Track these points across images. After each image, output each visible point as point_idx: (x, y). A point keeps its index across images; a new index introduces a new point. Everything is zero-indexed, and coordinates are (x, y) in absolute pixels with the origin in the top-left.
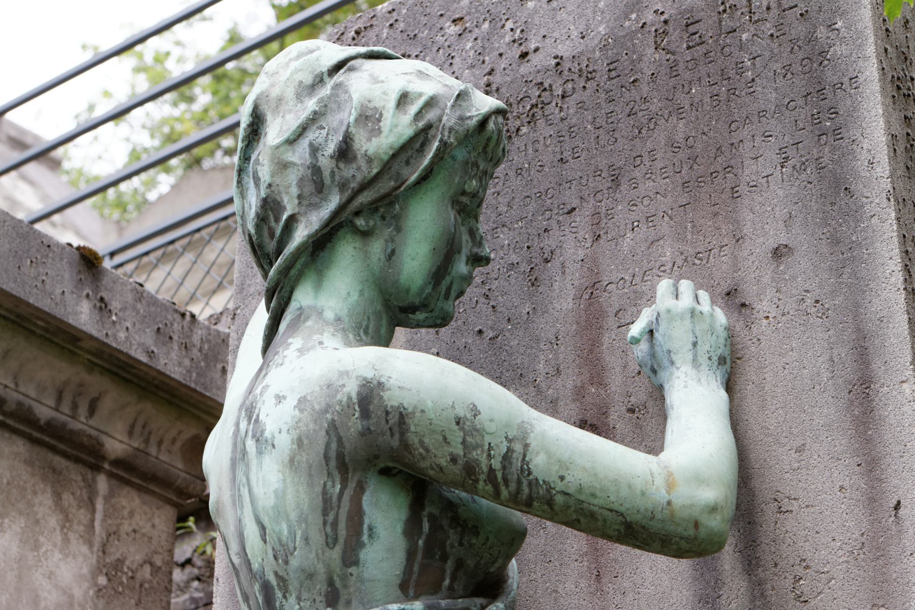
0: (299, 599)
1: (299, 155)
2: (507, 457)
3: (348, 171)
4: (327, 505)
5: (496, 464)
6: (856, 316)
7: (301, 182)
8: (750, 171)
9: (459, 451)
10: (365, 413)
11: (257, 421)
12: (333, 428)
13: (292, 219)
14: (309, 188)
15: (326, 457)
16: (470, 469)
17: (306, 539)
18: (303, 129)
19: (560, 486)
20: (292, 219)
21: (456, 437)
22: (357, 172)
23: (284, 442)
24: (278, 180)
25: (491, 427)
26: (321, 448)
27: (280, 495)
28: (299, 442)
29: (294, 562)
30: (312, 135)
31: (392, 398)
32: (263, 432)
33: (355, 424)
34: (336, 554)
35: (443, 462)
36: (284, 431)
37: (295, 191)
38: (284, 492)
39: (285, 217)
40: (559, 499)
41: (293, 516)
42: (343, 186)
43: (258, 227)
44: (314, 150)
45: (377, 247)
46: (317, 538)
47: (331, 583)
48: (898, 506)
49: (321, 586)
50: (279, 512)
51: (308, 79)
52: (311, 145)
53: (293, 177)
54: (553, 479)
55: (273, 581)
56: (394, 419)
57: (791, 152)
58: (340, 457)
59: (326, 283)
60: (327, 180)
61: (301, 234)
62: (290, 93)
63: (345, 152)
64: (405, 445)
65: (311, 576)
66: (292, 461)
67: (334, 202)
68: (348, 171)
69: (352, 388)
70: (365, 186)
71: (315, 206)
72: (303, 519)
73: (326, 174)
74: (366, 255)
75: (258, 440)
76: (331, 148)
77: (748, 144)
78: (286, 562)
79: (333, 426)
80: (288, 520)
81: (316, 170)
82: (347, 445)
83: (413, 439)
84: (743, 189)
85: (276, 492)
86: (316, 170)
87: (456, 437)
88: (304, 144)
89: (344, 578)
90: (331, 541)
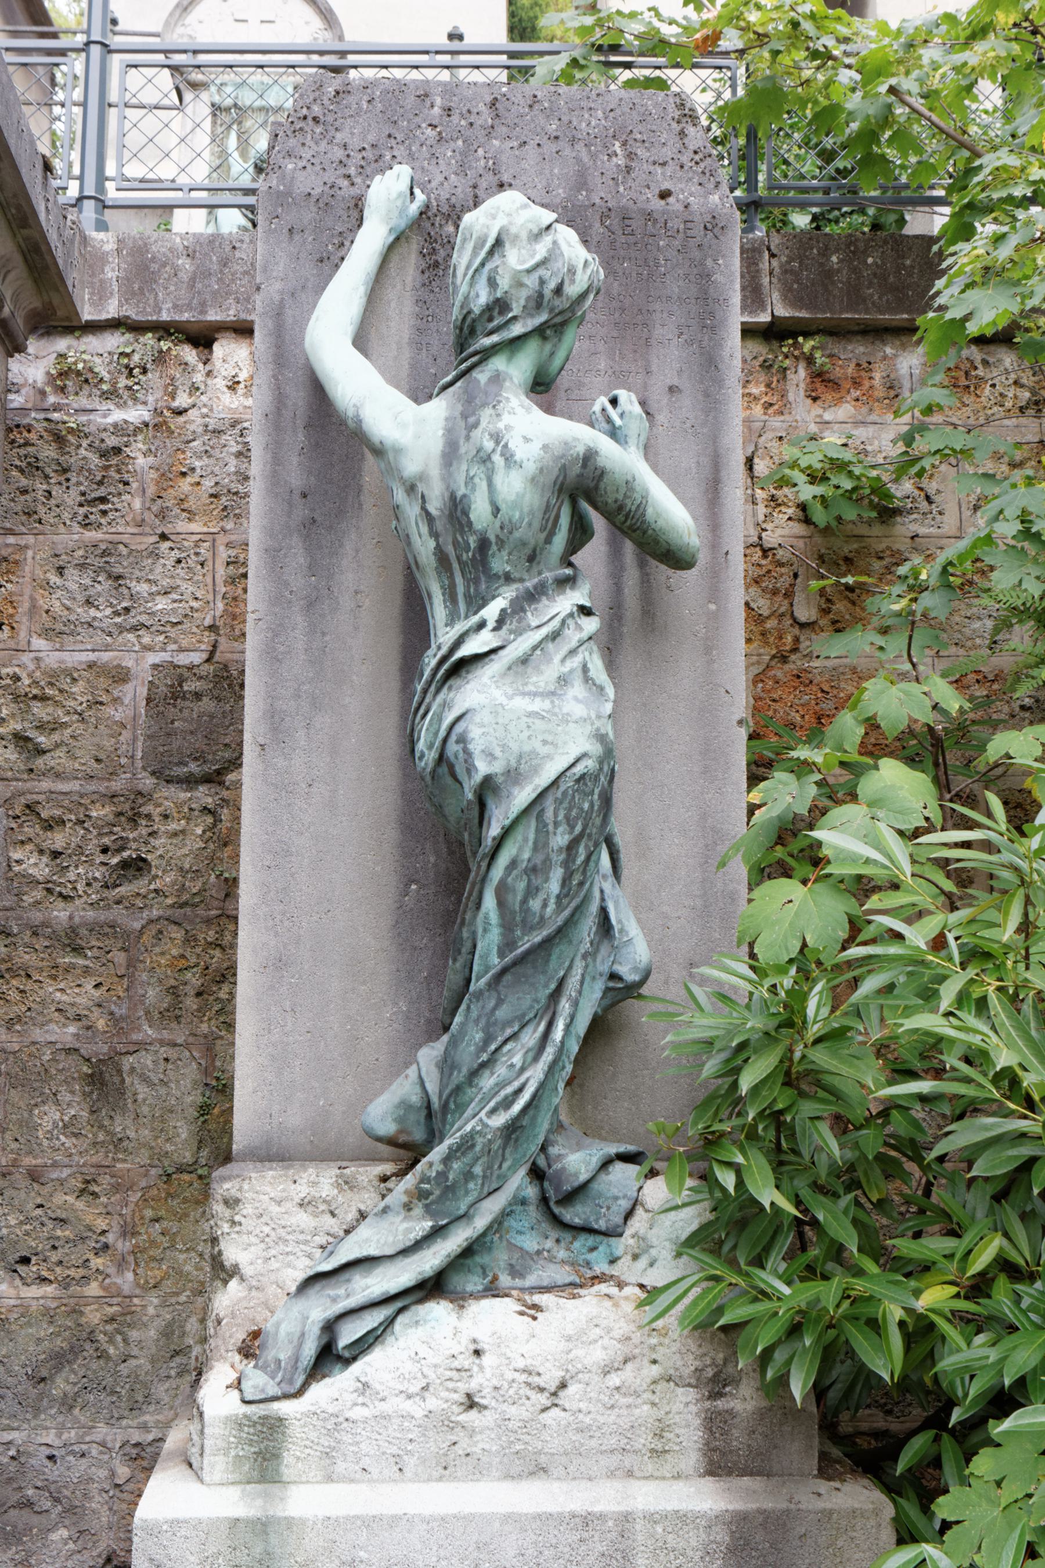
0: (510, 554)
1: (532, 281)
2: (639, 506)
3: (557, 302)
4: (547, 509)
5: (633, 508)
6: (715, 442)
7: (528, 299)
8: (658, 332)
9: (620, 497)
10: (584, 465)
11: (506, 446)
12: (564, 468)
13: (515, 318)
14: (532, 304)
15: (555, 483)
16: (621, 508)
17: (530, 525)
18: (537, 266)
19: (653, 526)
20: (515, 318)
21: (623, 490)
22: (561, 304)
23: (531, 467)
24: (513, 291)
25: (638, 489)
26: (553, 478)
27: (520, 496)
28: (541, 470)
29: (517, 534)
30: (541, 272)
31: (601, 462)
32: (512, 456)
33: (576, 469)
34: (543, 536)
35: (610, 501)
36: (532, 459)
37: (522, 302)
38: (523, 495)
39: (510, 315)
40: (650, 532)
41: (526, 510)
42: (551, 310)
43: (483, 312)
44: (542, 282)
45: (548, 347)
46: (536, 524)
47: (534, 550)
48: (727, 553)
49: (528, 551)
50: (515, 505)
51: (536, 231)
52: (540, 278)
53: (524, 294)
54: (652, 521)
55: (493, 539)
56: (598, 473)
57: (685, 330)
58: (562, 484)
59: (514, 360)
60: (545, 303)
61: (517, 330)
62: (524, 235)
63: (558, 291)
64: (596, 488)
65: (524, 544)
66: (533, 479)
67: (543, 317)
68: (557, 302)
69: (581, 450)
70: (561, 313)
71: (532, 316)
72: (531, 513)
73: (546, 299)
74: (542, 350)
75: (507, 459)
76: (552, 285)
77: (658, 314)
78: (511, 533)
79: (564, 467)
80: (521, 512)
81: (541, 295)
82: (568, 480)
83: (602, 485)
84: (653, 342)
85: (517, 494)
86: (541, 295)
87: (623, 490)
88: (535, 276)
89: (542, 549)
90: (542, 529)
